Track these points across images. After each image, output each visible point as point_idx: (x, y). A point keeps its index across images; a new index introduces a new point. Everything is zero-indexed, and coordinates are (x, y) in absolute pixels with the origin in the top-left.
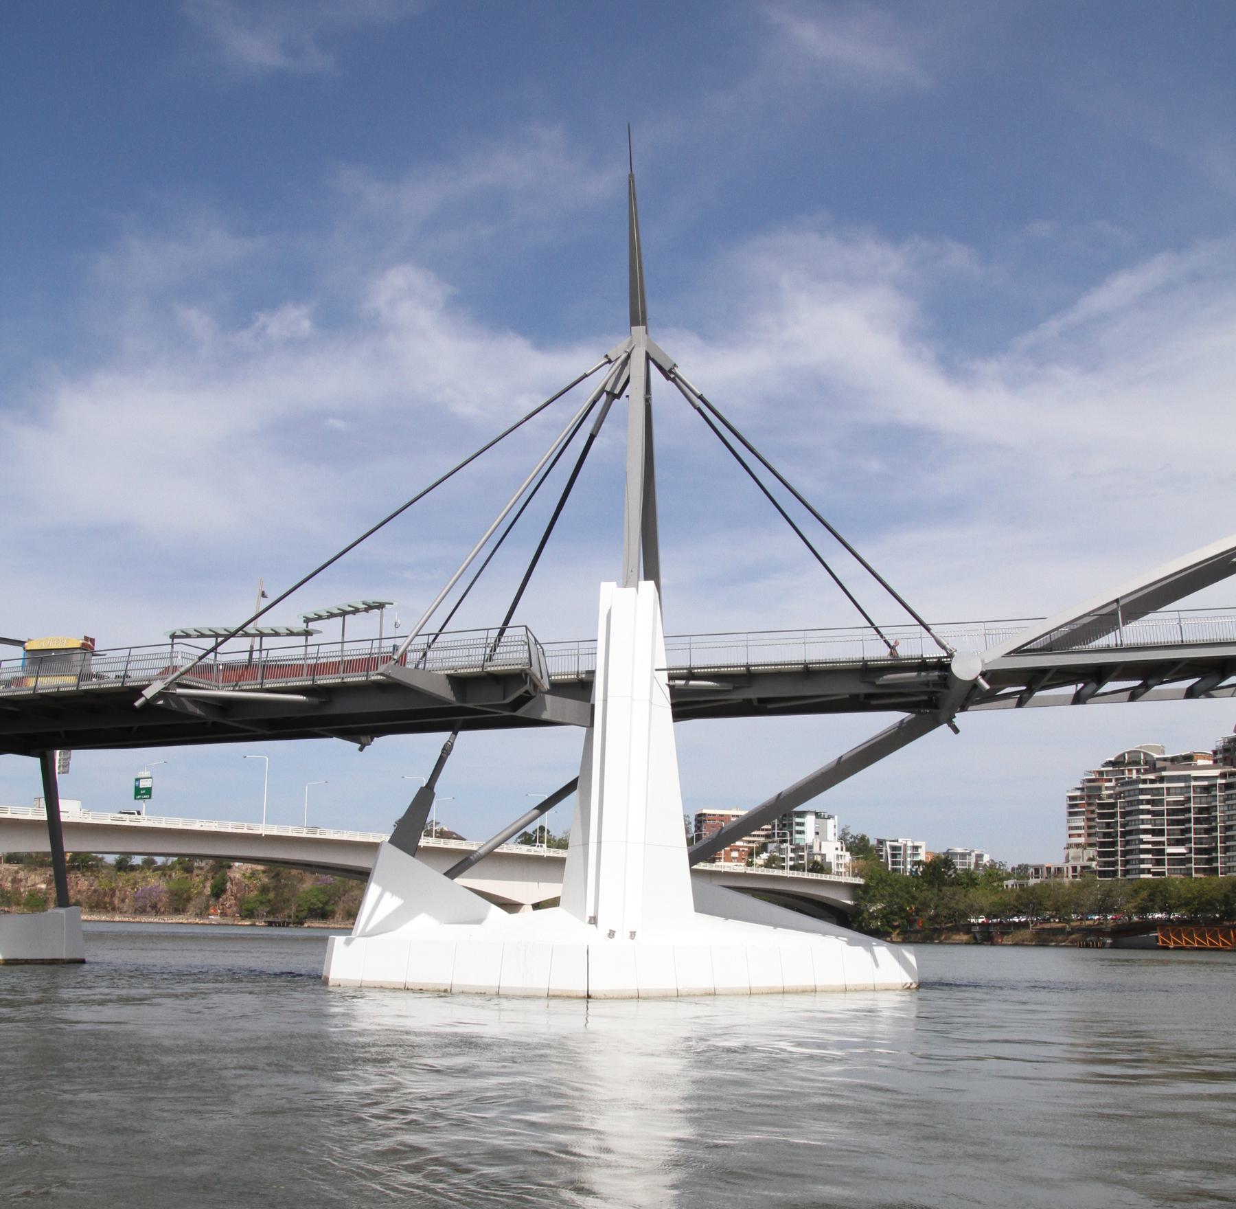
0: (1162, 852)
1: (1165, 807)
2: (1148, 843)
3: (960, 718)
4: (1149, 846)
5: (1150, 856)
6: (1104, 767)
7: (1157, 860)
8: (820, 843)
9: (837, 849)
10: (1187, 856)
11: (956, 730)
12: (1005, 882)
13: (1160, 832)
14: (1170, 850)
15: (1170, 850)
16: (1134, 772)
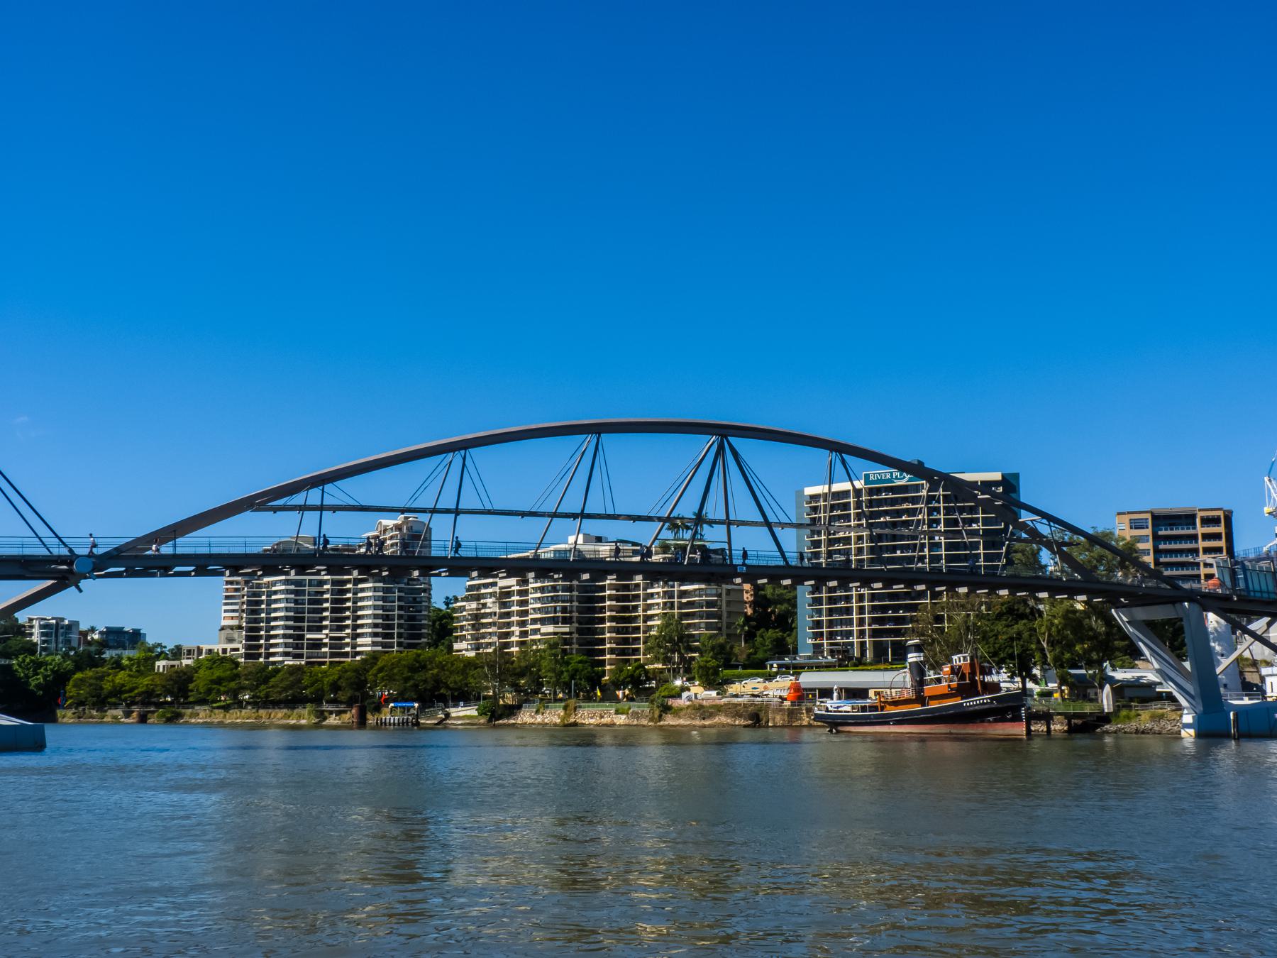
0: (301, 637)
1: (307, 597)
3: (83, 583)
4: (291, 632)
5: (291, 641)
7: (297, 644)
11: (80, 591)
12: (157, 663)
15: (308, 636)
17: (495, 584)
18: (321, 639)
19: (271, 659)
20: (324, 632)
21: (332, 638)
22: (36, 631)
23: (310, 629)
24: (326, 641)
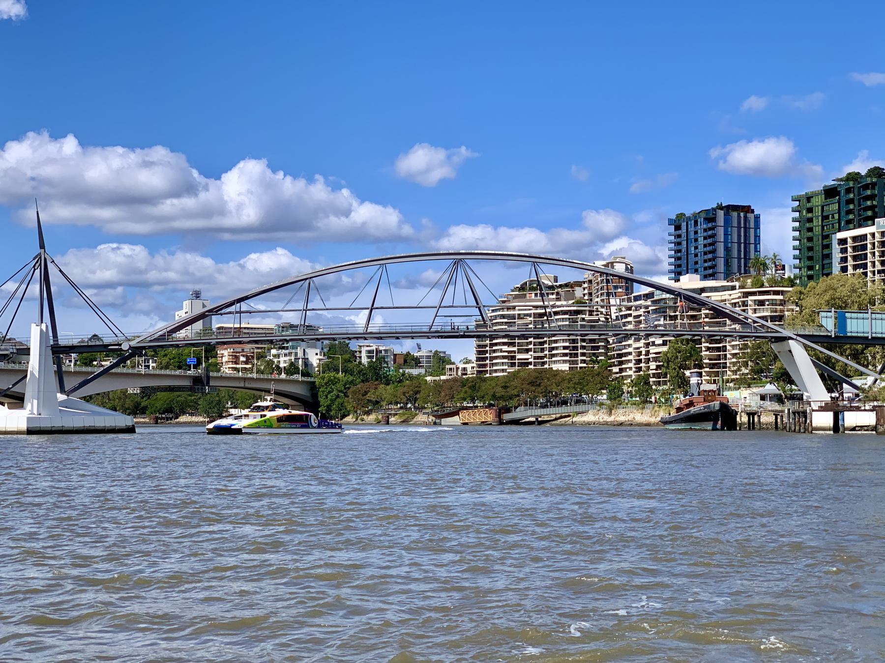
0: (513, 358)
2: (501, 351)
4: (506, 354)
5: (506, 361)
6: (513, 291)
8: (304, 350)
9: (317, 354)
10: (530, 360)
13: (513, 344)
14: (519, 356)
15: (519, 356)
16: (533, 295)
17: (630, 315)
18: (528, 359)
19: (495, 375)
20: (530, 353)
21: (535, 358)
22: (364, 355)
23: (520, 351)
24: (532, 360)
